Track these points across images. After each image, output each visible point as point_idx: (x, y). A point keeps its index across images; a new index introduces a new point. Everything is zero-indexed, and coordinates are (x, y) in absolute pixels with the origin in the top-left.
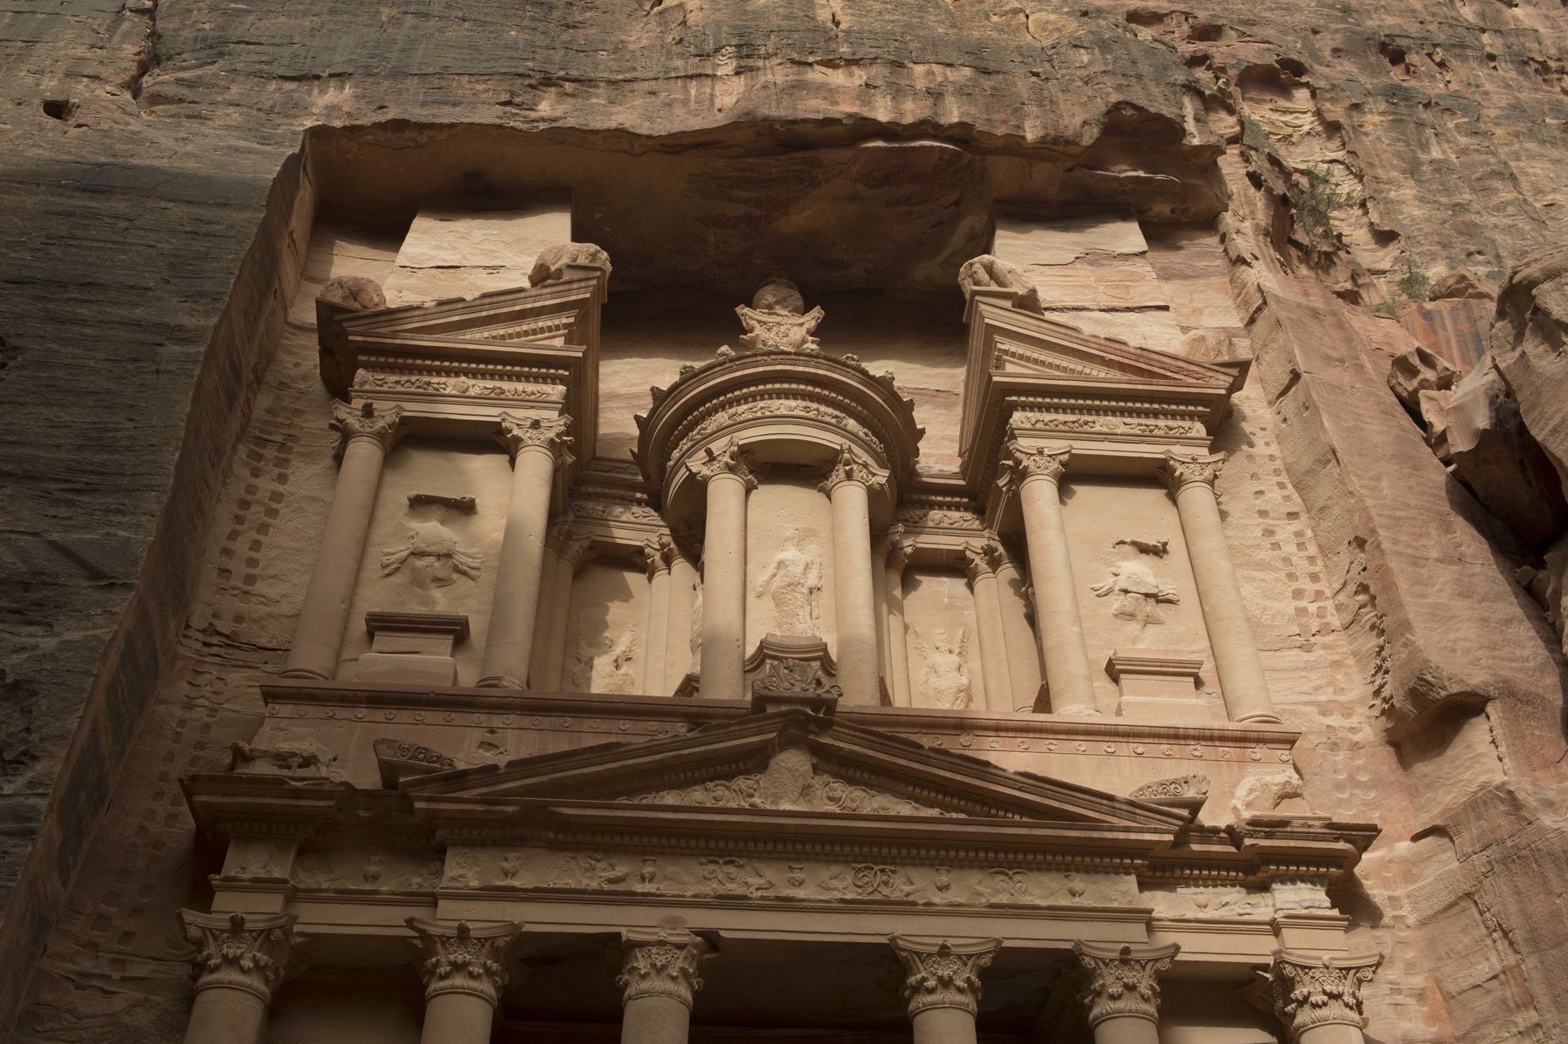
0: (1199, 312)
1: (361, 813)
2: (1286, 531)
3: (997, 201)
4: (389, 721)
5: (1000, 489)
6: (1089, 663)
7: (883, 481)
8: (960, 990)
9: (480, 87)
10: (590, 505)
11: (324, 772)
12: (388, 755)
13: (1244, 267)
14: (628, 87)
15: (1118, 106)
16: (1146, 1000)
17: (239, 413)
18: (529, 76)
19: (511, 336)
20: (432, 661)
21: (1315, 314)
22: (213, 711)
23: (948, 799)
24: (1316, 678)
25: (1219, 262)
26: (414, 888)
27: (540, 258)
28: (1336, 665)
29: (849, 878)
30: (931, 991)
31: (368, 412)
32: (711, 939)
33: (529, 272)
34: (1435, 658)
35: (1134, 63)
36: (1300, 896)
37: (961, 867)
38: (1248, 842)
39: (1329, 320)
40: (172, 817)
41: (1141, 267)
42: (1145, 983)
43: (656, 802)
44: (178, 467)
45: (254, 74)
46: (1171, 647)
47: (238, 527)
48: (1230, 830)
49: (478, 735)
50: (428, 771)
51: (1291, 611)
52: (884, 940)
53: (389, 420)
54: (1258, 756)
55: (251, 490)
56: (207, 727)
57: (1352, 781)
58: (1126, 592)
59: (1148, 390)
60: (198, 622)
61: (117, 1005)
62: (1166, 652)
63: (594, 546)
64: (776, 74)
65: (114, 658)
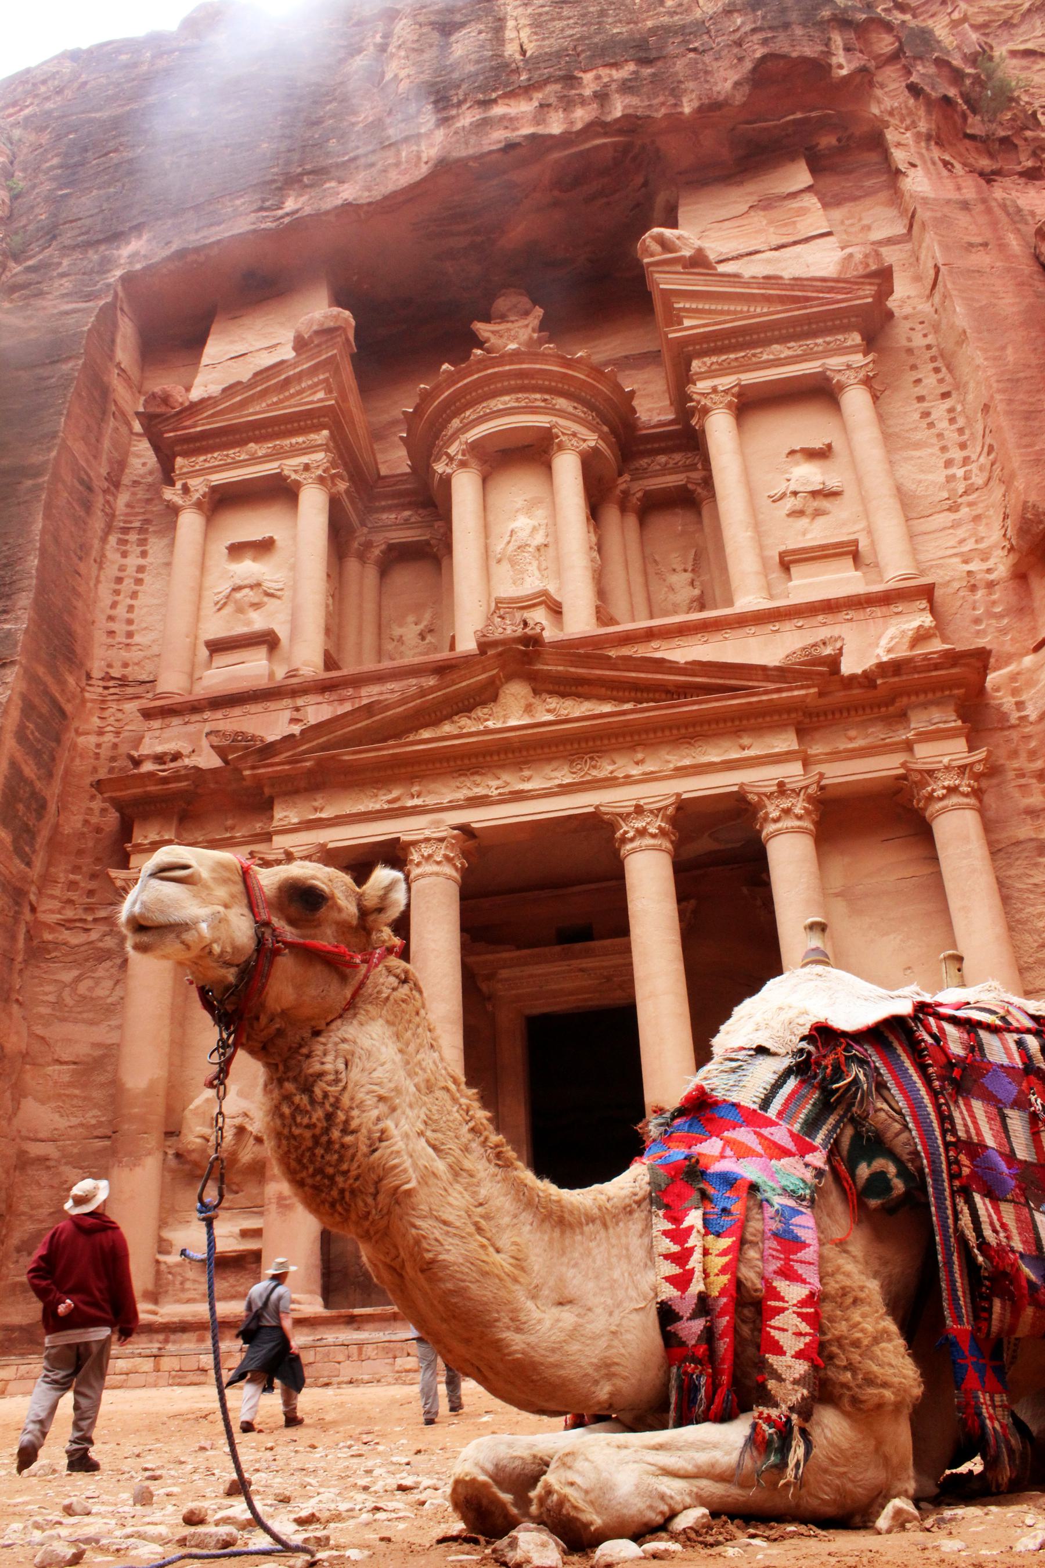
0: (868, 228)
1: (212, 786)
2: (940, 410)
3: (680, 173)
4: (226, 717)
5: (693, 427)
7: (592, 444)
8: (654, 836)
9: (238, 202)
10: (384, 516)
11: (187, 761)
12: (216, 741)
13: (901, 177)
14: (353, 165)
16: (799, 818)
17: (100, 514)
18: (273, 181)
19: (281, 401)
20: (252, 668)
21: (965, 206)
22: (117, 733)
23: (639, 695)
24: (961, 533)
25: (884, 178)
26: (258, 831)
27: (297, 331)
28: (977, 519)
29: (566, 769)
30: (632, 840)
31: (186, 489)
32: (465, 830)
33: (291, 344)
34: (1033, 498)
37: (652, 744)
39: (980, 207)
40: (103, 811)
43: (418, 738)
44: (41, 569)
45: (77, 246)
47: (116, 598)
48: (864, 672)
49: (287, 714)
50: (247, 748)
51: (942, 479)
52: (591, 809)
53: (201, 492)
54: (900, 609)
55: (122, 568)
56: (115, 746)
58: (795, 493)
59: (807, 314)
60: (97, 674)
61: (94, 936)
63: (391, 548)
64: (468, 117)
65: (15, 714)
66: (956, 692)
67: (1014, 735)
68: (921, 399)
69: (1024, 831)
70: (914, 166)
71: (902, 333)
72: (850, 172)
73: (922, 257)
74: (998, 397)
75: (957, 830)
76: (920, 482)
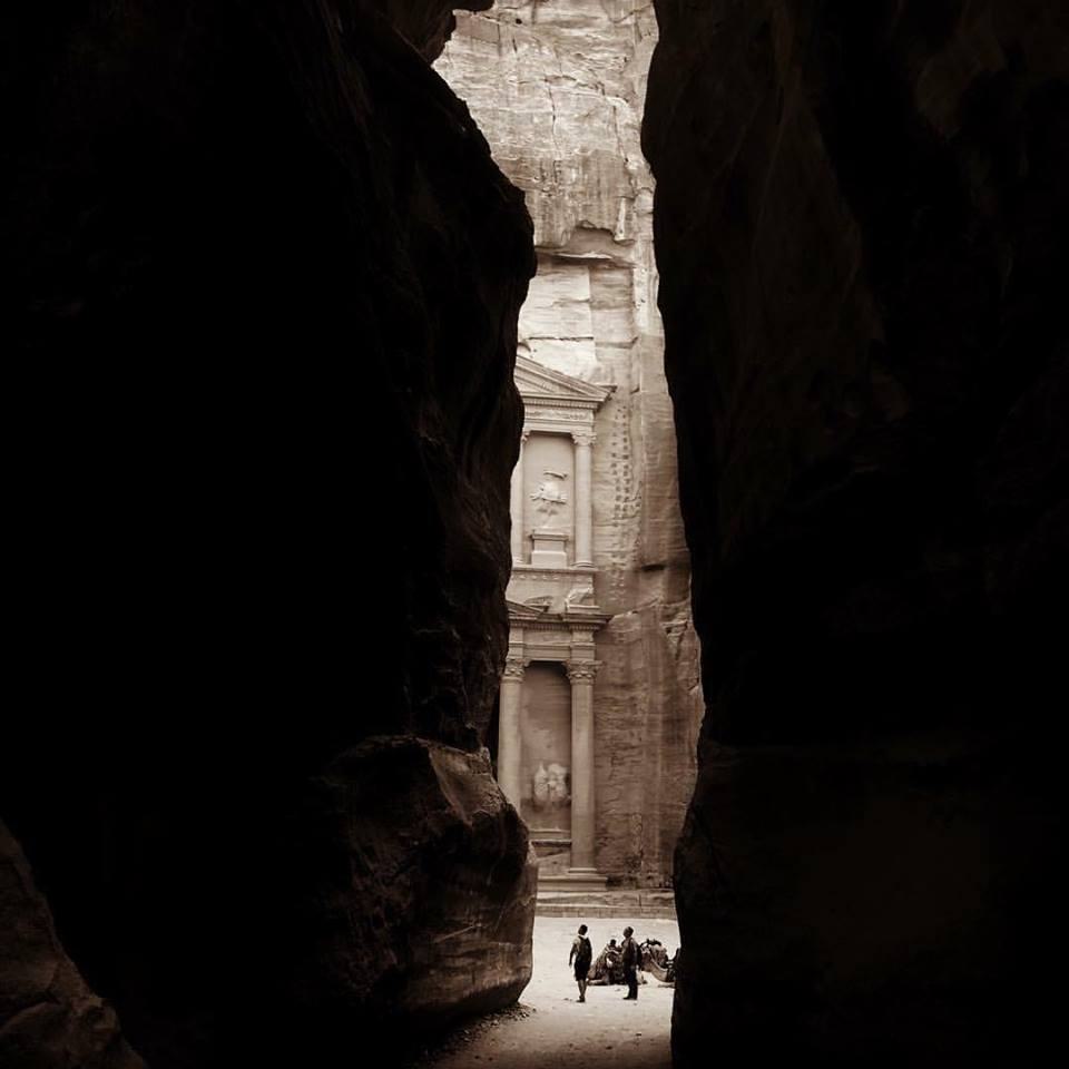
0: (611, 331)
6: (524, 533)
15: (582, 222)
16: (518, 676)
24: (616, 540)
25: (627, 298)
28: (624, 534)
35: (599, 181)
36: (582, 638)
38: (565, 620)
41: (586, 309)
42: (518, 670)
46: (559, 527)
48: (559, 615)
51: (613, 506)
57: (618, 587)
62: (554, 530)
66: (596, 628)
67: (614, 648)
68: (614, 455)
69: (610, 693)
70: (643, 301)
71: (614, 415)
72: (610, 286)
73: (634, 369)
74: (647, 486)
75: (582, 692)
76: (603, 505)
